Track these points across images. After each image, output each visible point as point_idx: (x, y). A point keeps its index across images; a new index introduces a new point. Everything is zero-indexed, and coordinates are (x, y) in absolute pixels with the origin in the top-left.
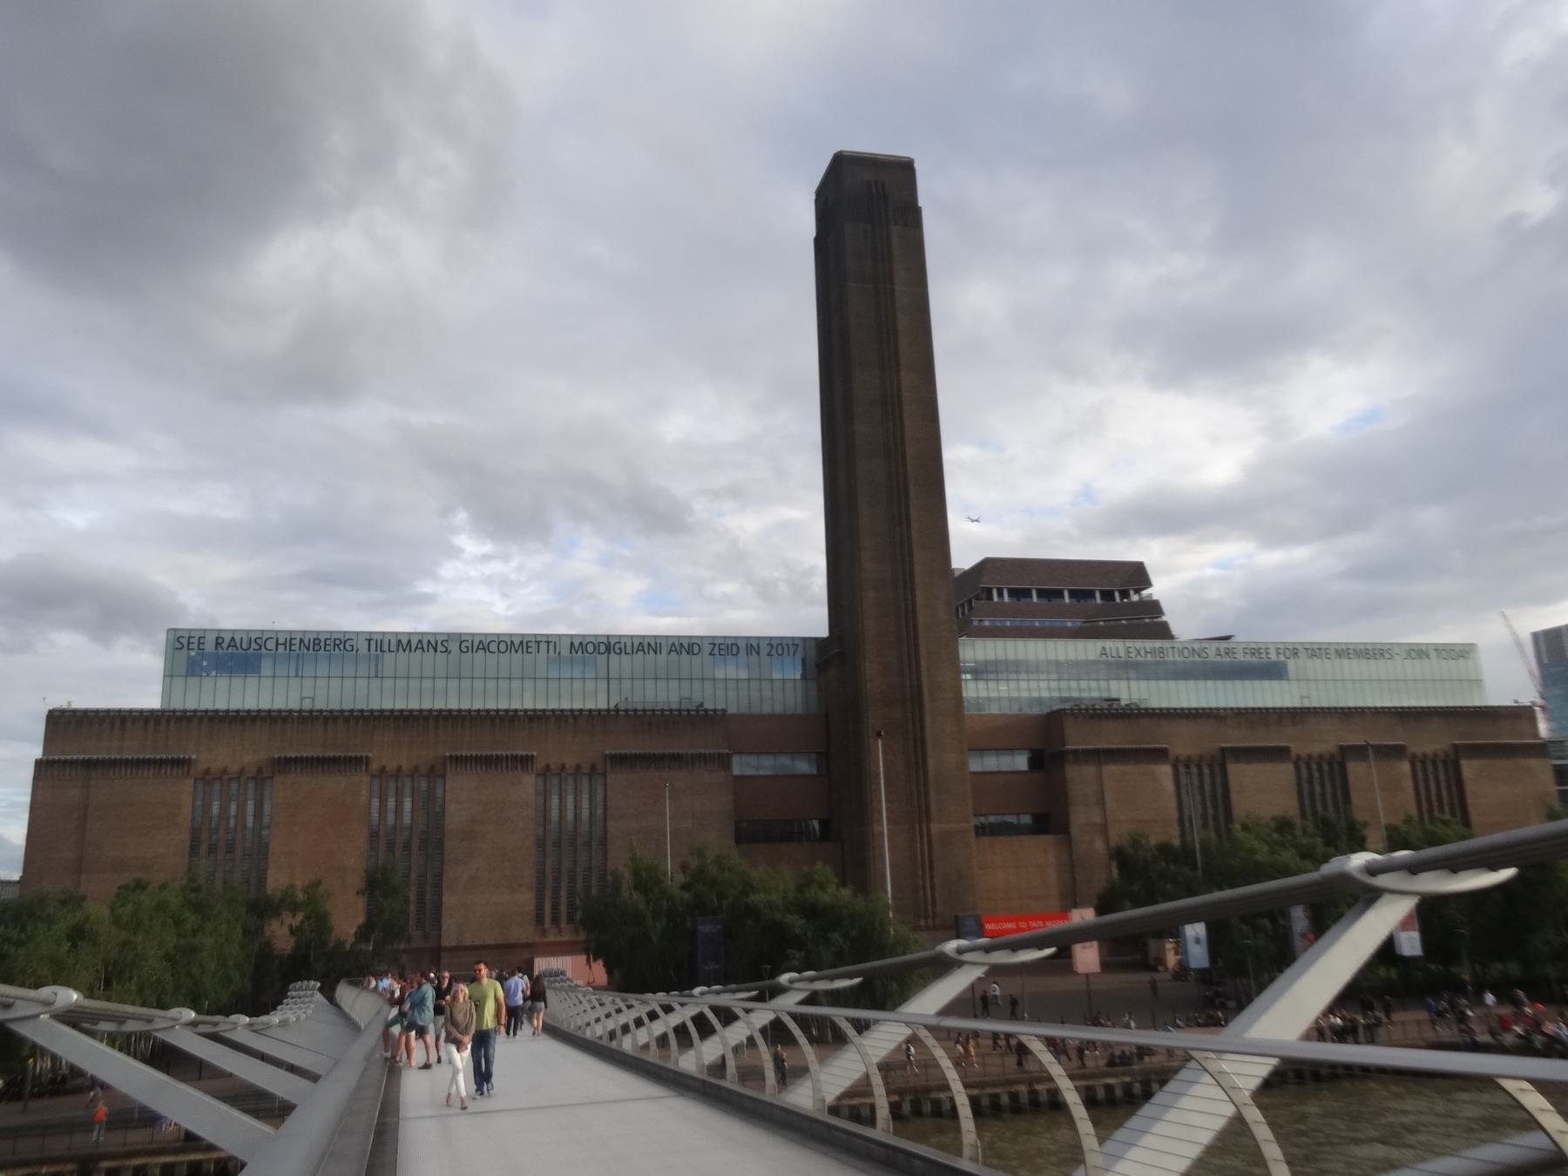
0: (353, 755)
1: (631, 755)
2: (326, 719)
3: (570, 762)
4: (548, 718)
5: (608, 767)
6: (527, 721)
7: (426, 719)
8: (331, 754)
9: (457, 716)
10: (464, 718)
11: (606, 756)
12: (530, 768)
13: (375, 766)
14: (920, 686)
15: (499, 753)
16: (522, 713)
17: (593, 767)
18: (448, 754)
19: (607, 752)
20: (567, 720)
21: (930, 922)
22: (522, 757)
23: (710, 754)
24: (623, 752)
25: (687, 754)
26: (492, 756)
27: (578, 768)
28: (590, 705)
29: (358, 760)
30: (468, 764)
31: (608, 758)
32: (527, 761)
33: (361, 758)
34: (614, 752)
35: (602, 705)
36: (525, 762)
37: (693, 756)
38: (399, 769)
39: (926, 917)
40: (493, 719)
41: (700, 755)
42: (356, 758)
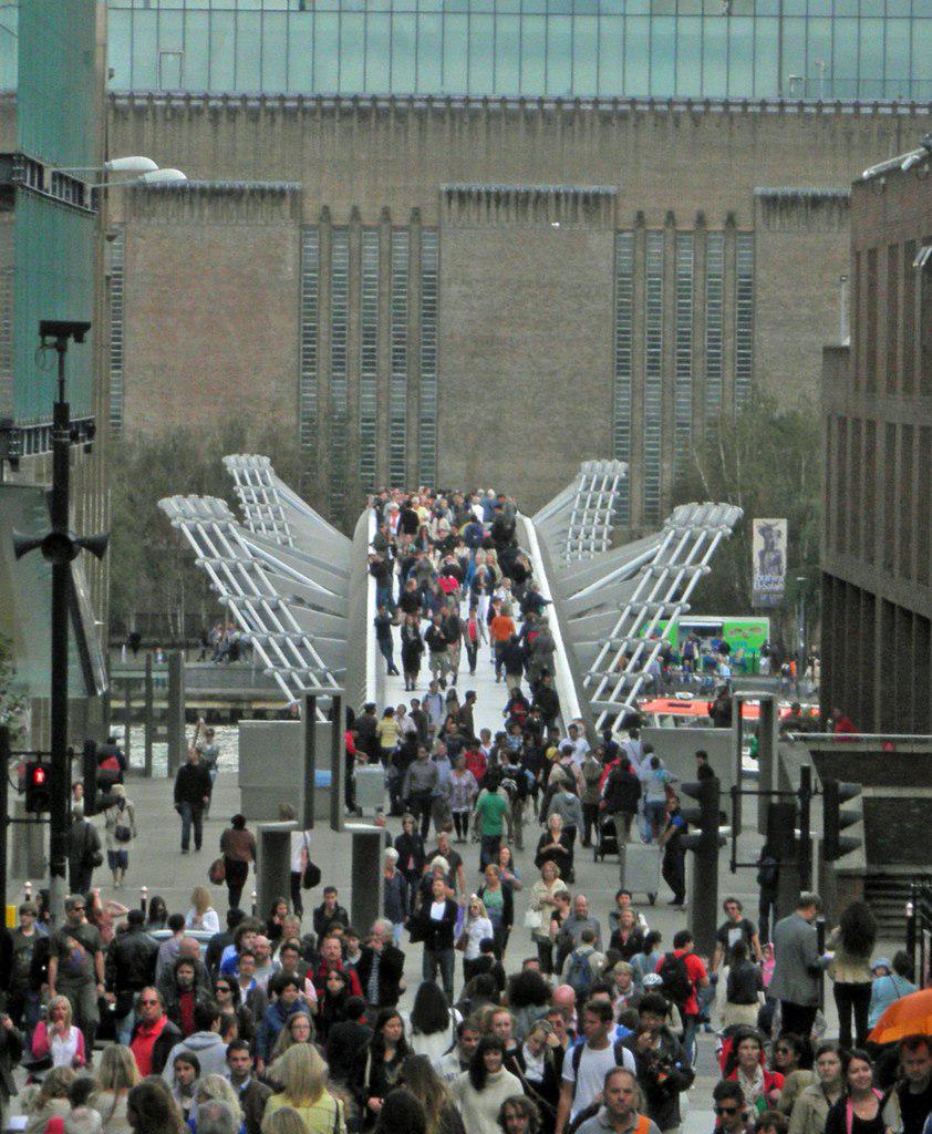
0: (266, 184)
2: (215, 112)
3: (686, 210)
4: (640, 116)
5: (759, 221)
6: (598, 123)
7: (401, 116)
8: (223, 182)
9: (461, 111)
10: (475, 115)
11: (756, 196)
12: (602, 216)
13: (311, 208)
15: (541, 187)
16: (589, 107)
17: (731, 220)
18: (444, 187)
19: (759, 190)
20: (677, 120)
22: (586, 197)
24: (789, 190)
26: (527, 193)
27: (701, 220)
28: (741, 89)
29: (278, 195)
30: (483, 209)
31: (758, 201)
32: (597, 204)
33: (282, 193)
34: (771, 191)
35: (767, 89)
36: (591, 203)
38: (355, 214)
40: (530, 117)
42: (272, 192)
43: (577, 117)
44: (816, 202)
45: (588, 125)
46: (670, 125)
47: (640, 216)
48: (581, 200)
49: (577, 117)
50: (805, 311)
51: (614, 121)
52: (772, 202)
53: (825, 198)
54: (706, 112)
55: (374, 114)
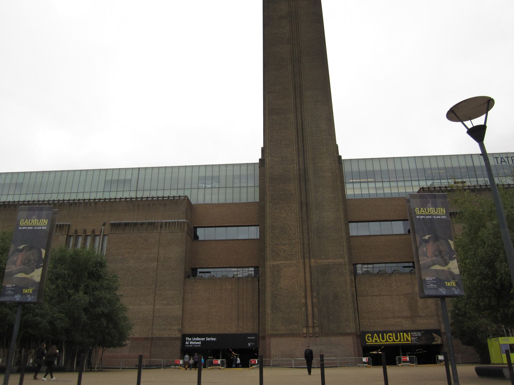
1: (123, 223)
4: (80, 203)
6: (68, 205)
14: (305, 170)
21: (311, 330)
22: (60, 225)
23: (173, 222)
25: (158, 222)
27: (93, 231)
32: (63, 227)
37: (162, 224)
39: (307, 327)
41: (166, 223)
43: (63, 204)
44: (126, 224)
45: (65, 207)
46: (88, 205)
47: (76, 231)
48: (59, 226)
49: (63, 204)
50: (120, 257)
51: (73, 205)
52: (113, 225)
53: (129, 223)
54: (99, 202)
55: (8, 206)
